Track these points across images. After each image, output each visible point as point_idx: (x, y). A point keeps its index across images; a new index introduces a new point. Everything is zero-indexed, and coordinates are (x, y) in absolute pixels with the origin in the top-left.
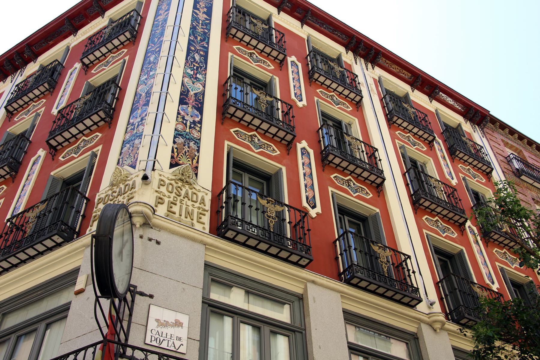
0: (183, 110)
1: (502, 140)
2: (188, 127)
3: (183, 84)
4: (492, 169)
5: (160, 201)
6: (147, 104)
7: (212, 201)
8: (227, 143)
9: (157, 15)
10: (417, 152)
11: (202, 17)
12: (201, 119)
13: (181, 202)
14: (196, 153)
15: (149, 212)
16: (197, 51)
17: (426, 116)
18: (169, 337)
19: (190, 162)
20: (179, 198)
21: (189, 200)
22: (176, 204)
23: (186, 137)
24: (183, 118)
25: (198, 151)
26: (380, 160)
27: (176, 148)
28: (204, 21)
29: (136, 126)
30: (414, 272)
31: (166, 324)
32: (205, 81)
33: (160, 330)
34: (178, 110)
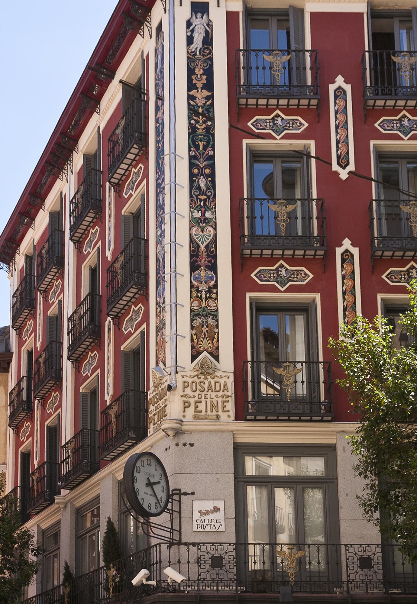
0: (196, 279)
2: (204, 300)
3: (192, 241)
5: (186, 405)
13: (205, 397)
14: (216, 330)
18: (210, 521)
19: (210, 345)
20: (203, 394)
21: (212, 392)
22: (201, 402)
23: (203, 315)
24: (198, 291)
25: (217, 326)
28: (204, 104)
31: (207, 513)
32: (216, 219)
33: (203, 518)
34: (191, 282)
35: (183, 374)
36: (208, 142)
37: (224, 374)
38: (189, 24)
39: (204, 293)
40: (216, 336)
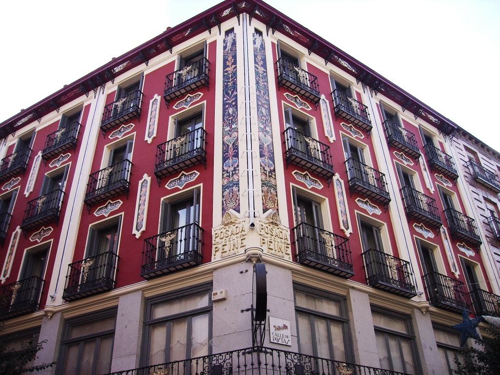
1: (465, 146)
4: (458, 176)
6: (236, 155)
7: (290, 235)
8: (291, 184)
9: (225, 66)
10: (407, 163)
11: (261, 69)
12: (274, 168)
14: (276, 198)
15: (259, 252)
16: (263, 105)
17: (414, 135)
19: (273, 206)
22: (271, 242)
23: (268, 186)
26: (387, 184)
27: (264, 196)
29: (231, 174)
30: (412, 274)
31: (279, 328)
33: (277, 332)
35: (260, 219)
36: (266, 92)
37: (285, 228)
38: (254, 36)
39: (267, 172)
40: (276, 202)
